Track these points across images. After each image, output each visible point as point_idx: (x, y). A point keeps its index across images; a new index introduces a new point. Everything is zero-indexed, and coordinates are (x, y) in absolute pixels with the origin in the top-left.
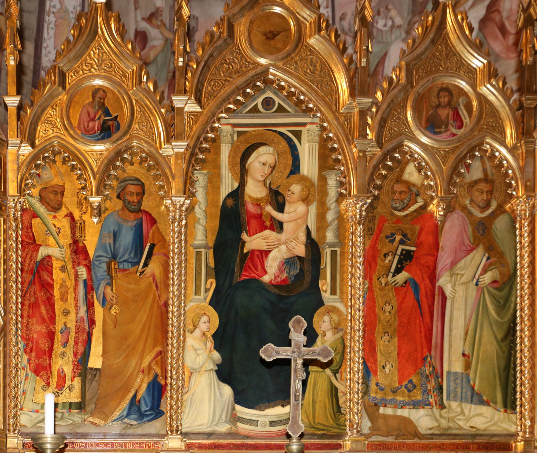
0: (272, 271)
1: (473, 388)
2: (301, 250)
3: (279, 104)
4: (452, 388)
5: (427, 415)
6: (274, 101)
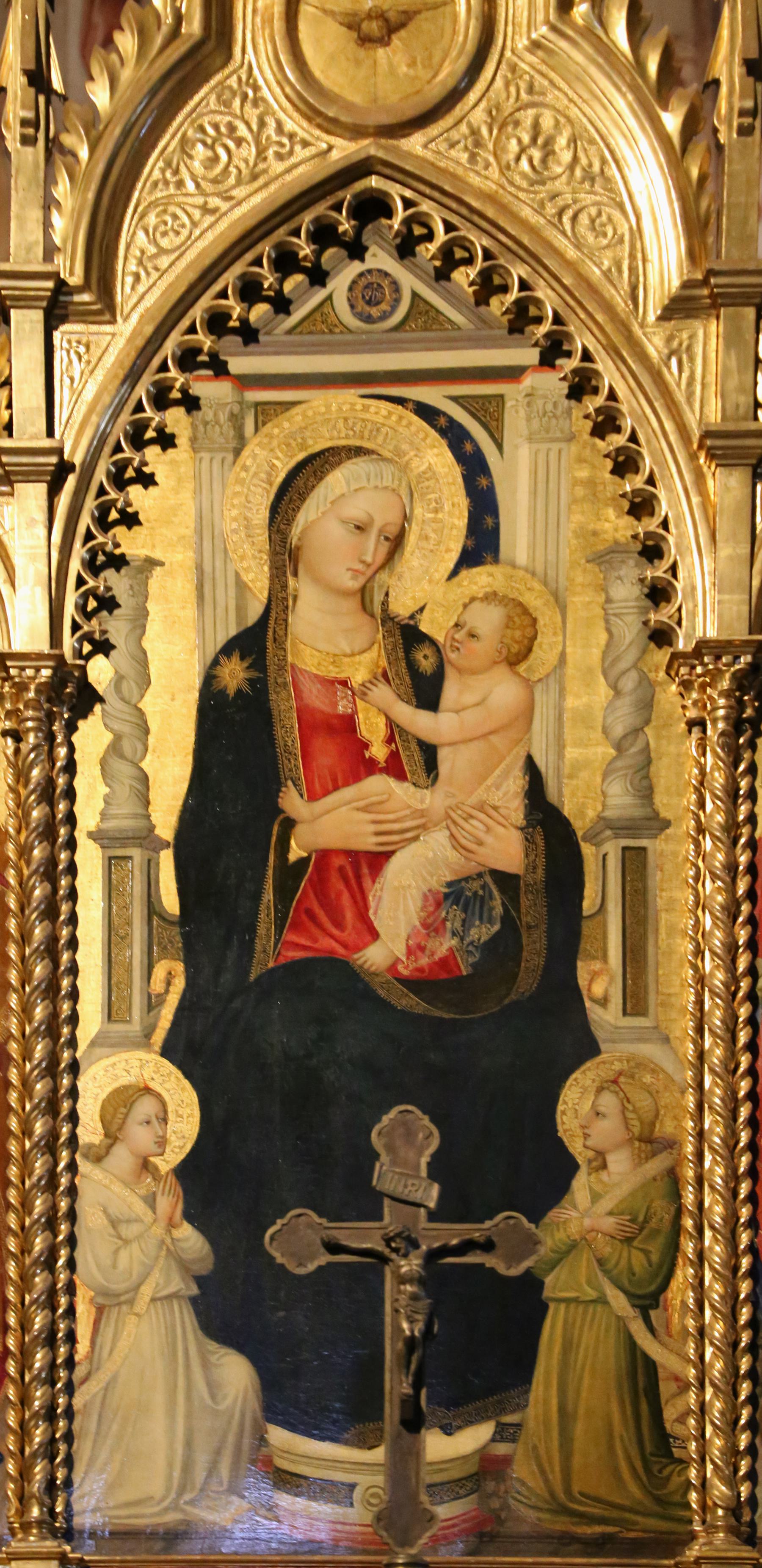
0: (396, 927)
2: (506, 847)
3: (415, 295)
6: (396, 287)
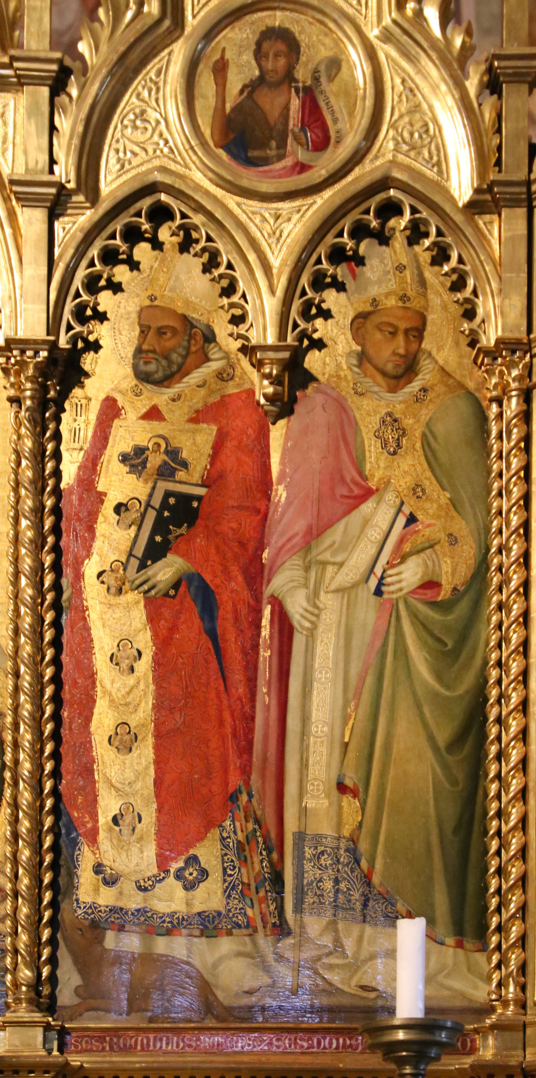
1: (367, 879)
4: (309, 877)
5: (239, 954)
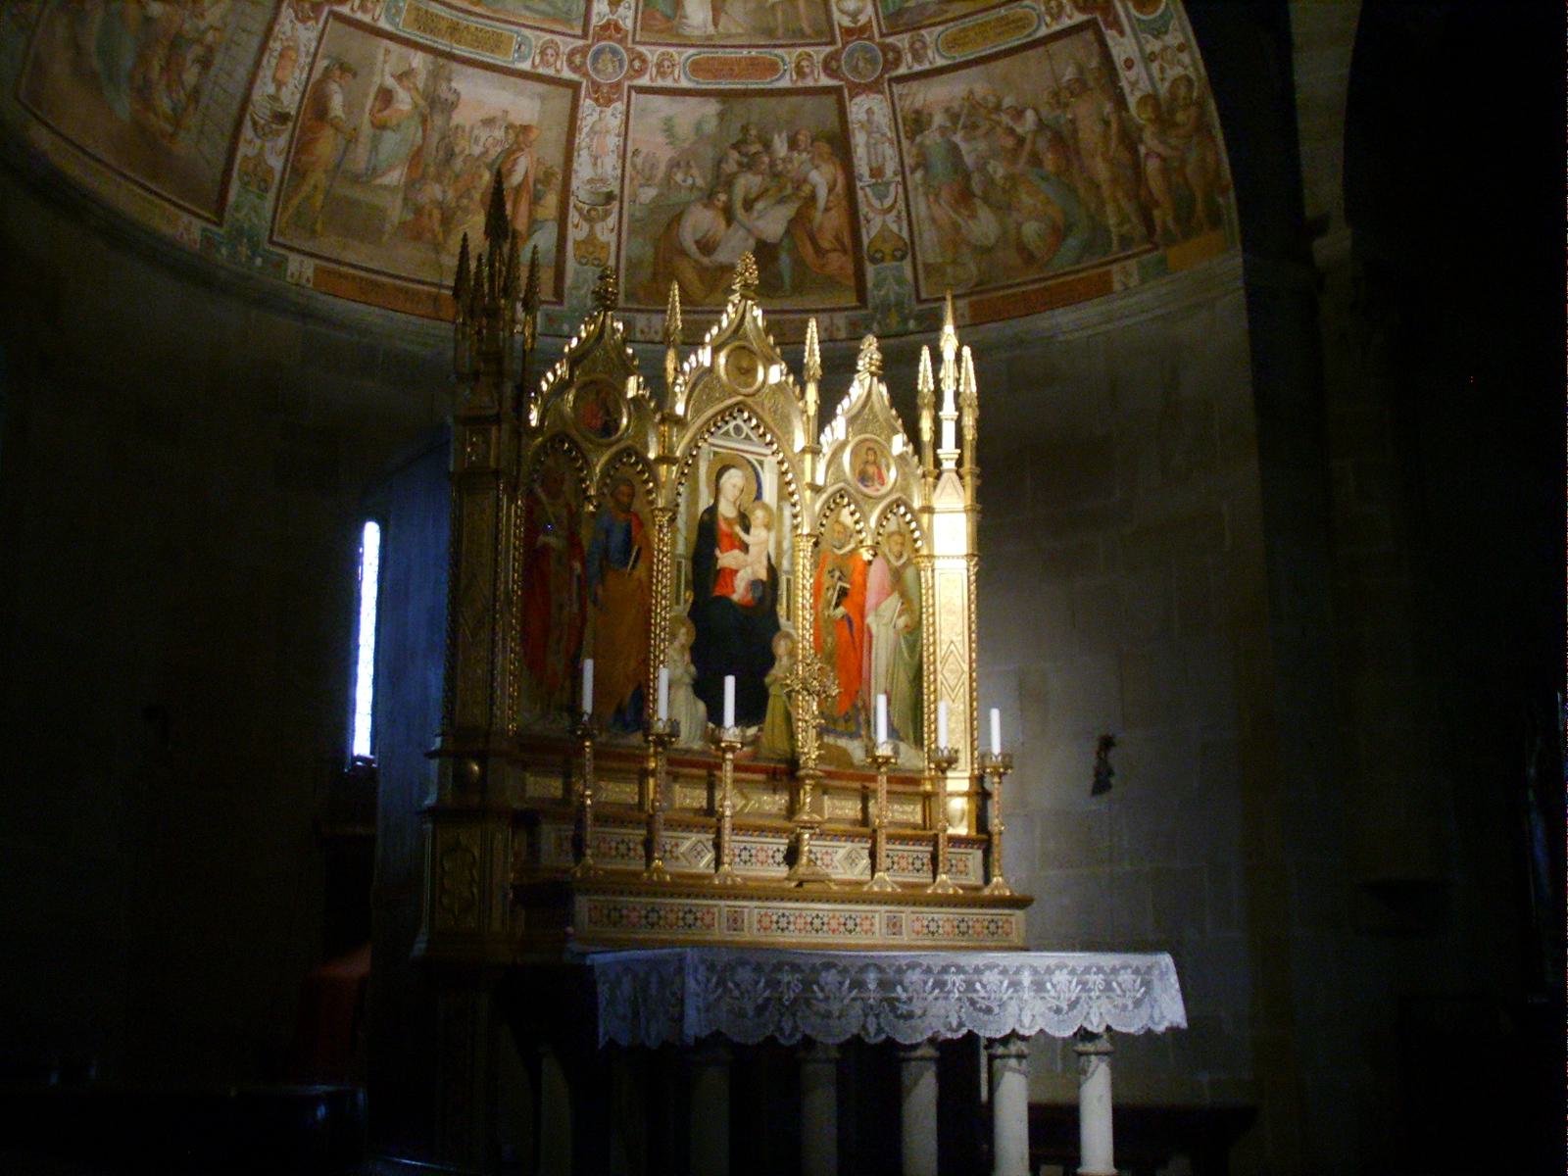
0: (740, 591)
2: (763, 575)
